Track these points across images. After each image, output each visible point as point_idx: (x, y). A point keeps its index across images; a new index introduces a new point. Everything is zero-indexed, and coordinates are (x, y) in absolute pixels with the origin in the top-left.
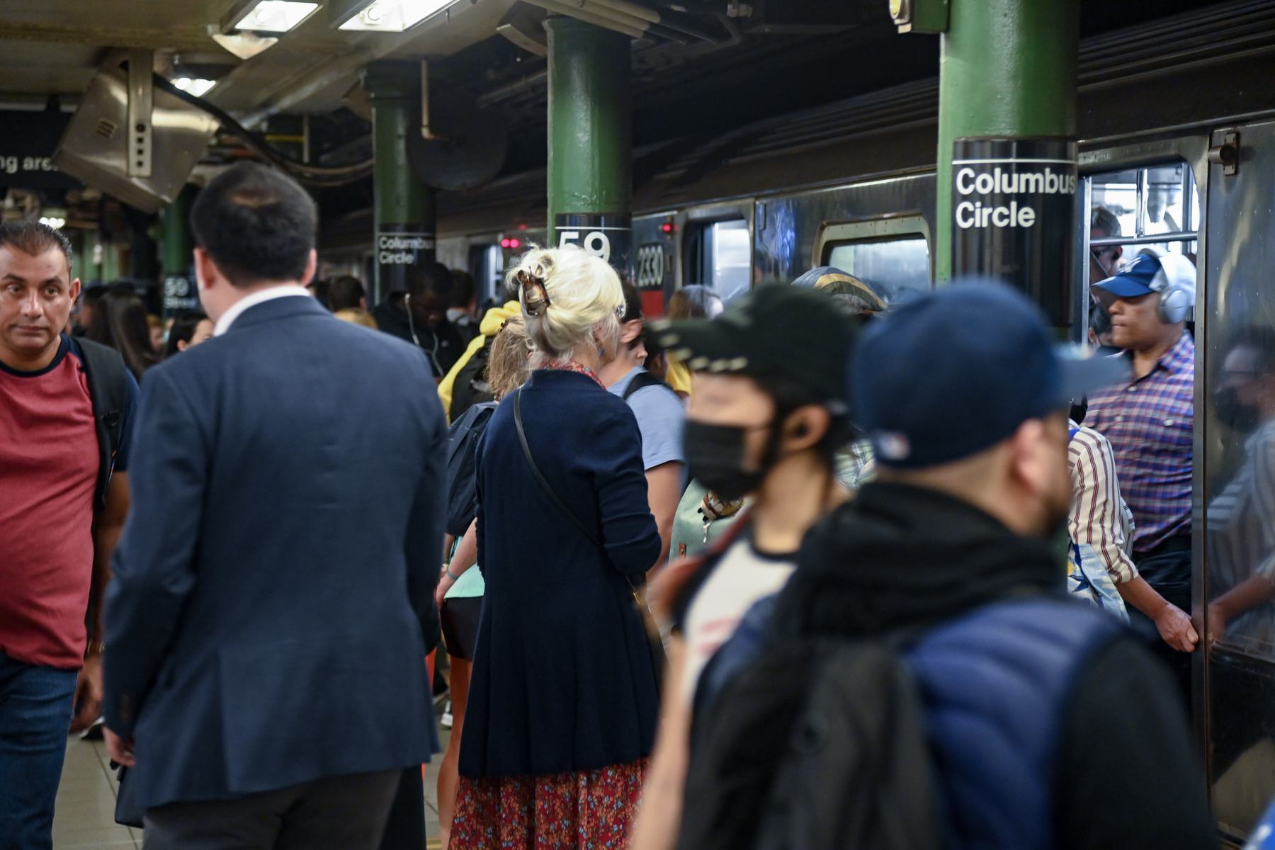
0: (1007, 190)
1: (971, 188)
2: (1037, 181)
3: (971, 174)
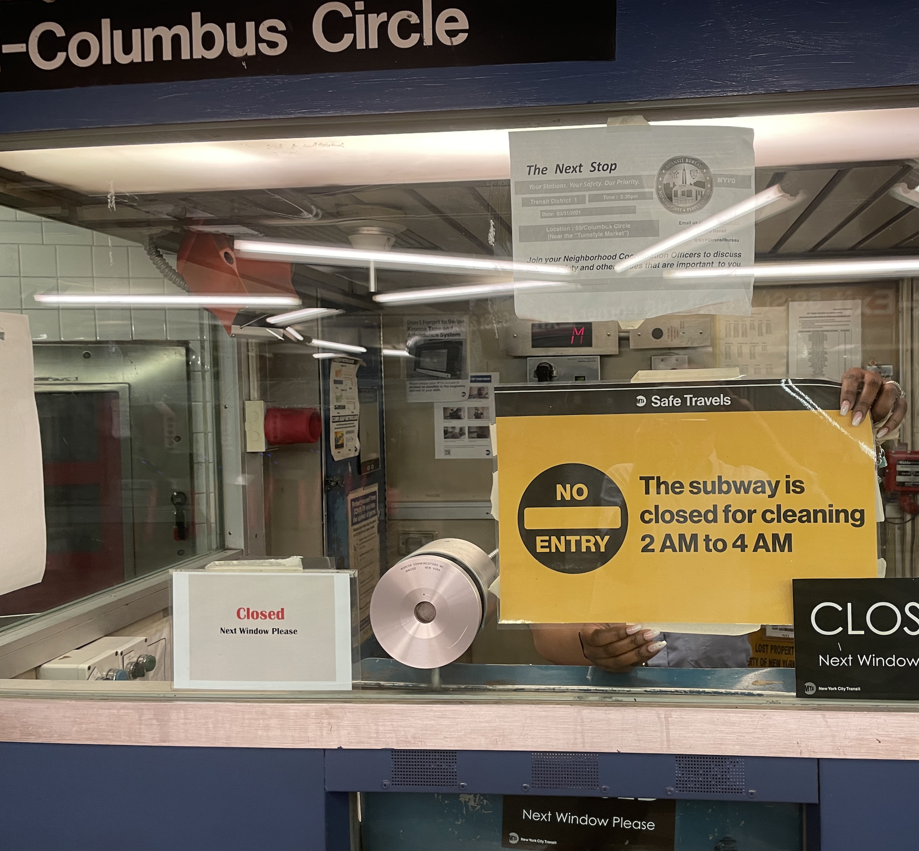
0: (123, 59)
2: (176, 39)
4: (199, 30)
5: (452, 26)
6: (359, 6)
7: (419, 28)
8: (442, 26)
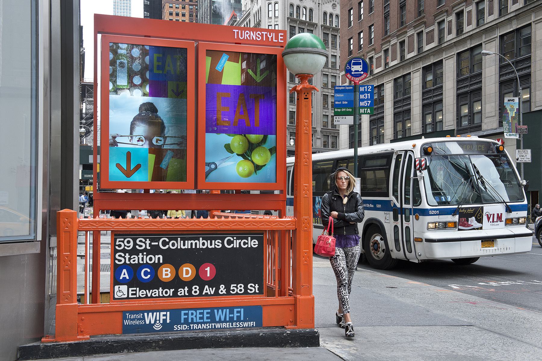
0: (183, 247)
1: (167, 246)
2: (196, 243)
3: (167, 240)
4: (201, 242)
5: (255, 243)
6: (235, 238)
7: (247, 243)
8: (252, 243)
